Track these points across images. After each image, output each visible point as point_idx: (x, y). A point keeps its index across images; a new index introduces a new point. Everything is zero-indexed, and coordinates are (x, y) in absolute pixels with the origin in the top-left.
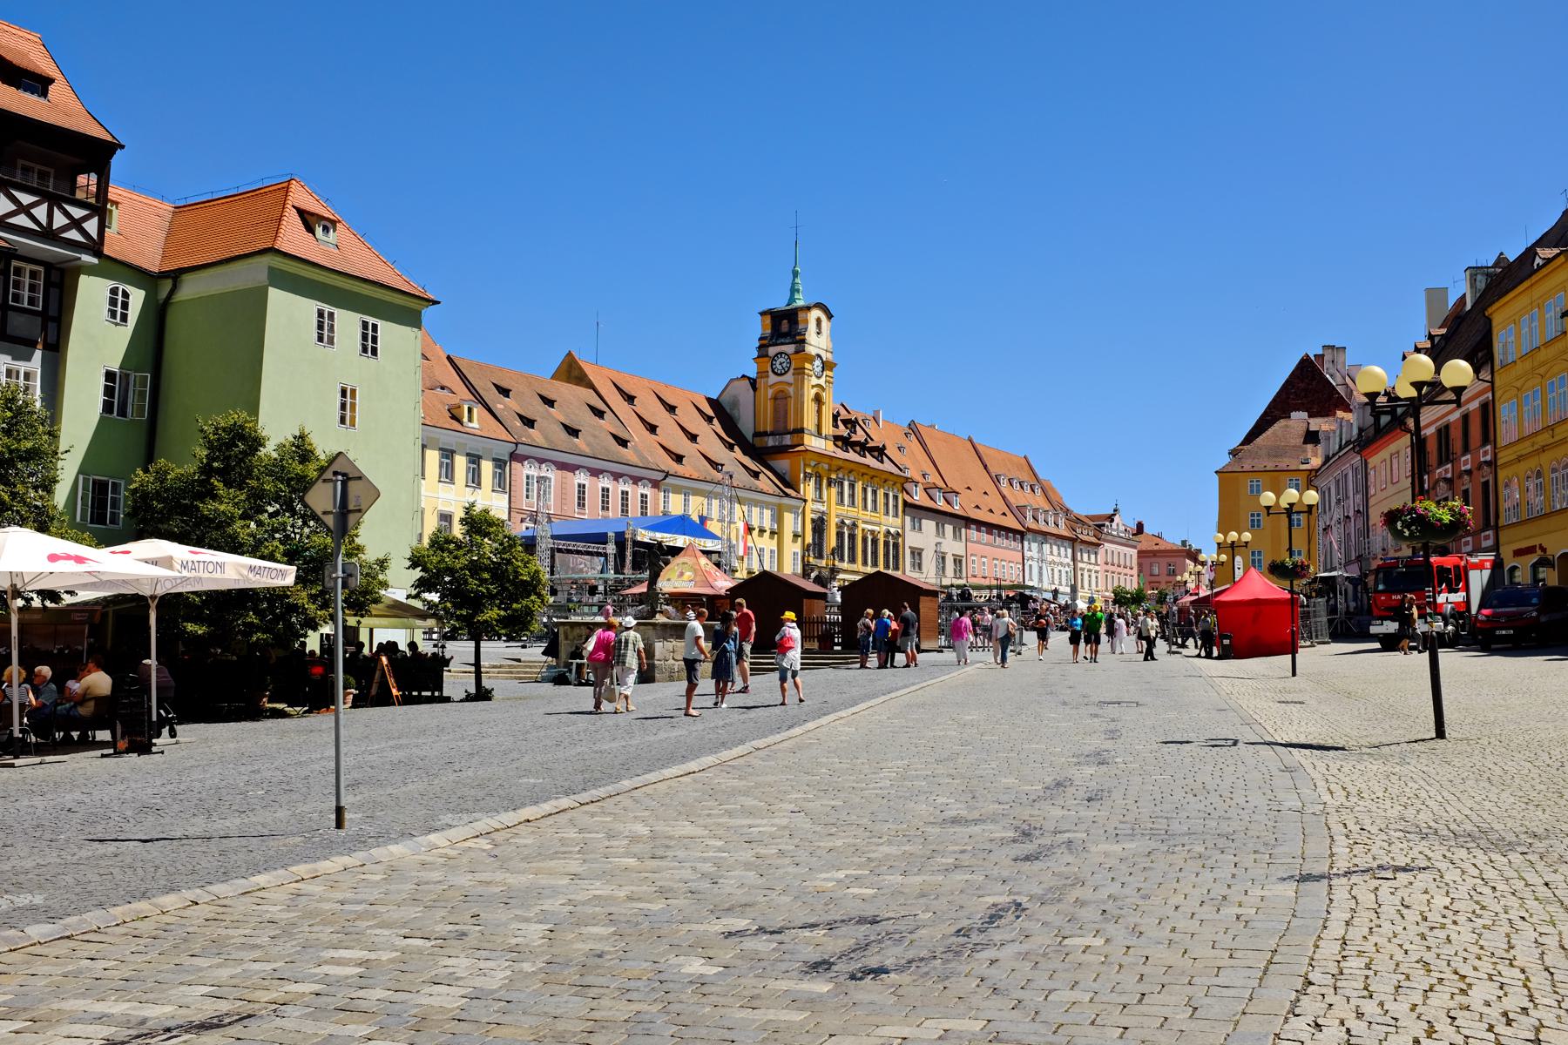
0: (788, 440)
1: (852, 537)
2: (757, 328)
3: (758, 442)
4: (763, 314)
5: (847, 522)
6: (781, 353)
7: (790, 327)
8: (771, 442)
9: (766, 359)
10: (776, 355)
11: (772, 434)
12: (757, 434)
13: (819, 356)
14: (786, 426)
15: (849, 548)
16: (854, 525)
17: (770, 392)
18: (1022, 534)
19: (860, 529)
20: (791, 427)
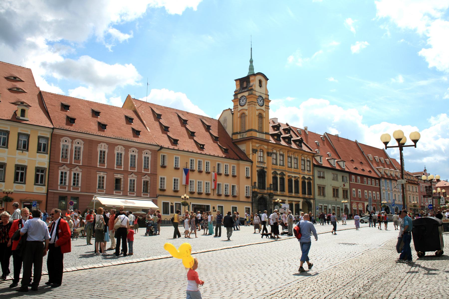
0: (246, 135)
1: (282, 179)
2: (233, 87)
3: (235, 137)
4: (236, 80)
5: (279, 172)
6: (243, 96)
7: (247, 84)
8: (239, 137)
9: (237, 100)
10: (241, 97)
11: (240, 133)
12: (234, 134)
13: (261, 96)
14: (245, 129)
15: (280, 185)
16: (282, 174)
17: (239, 114)
18: (379, 179)
19: (287, 176)
20: (247, 129)
